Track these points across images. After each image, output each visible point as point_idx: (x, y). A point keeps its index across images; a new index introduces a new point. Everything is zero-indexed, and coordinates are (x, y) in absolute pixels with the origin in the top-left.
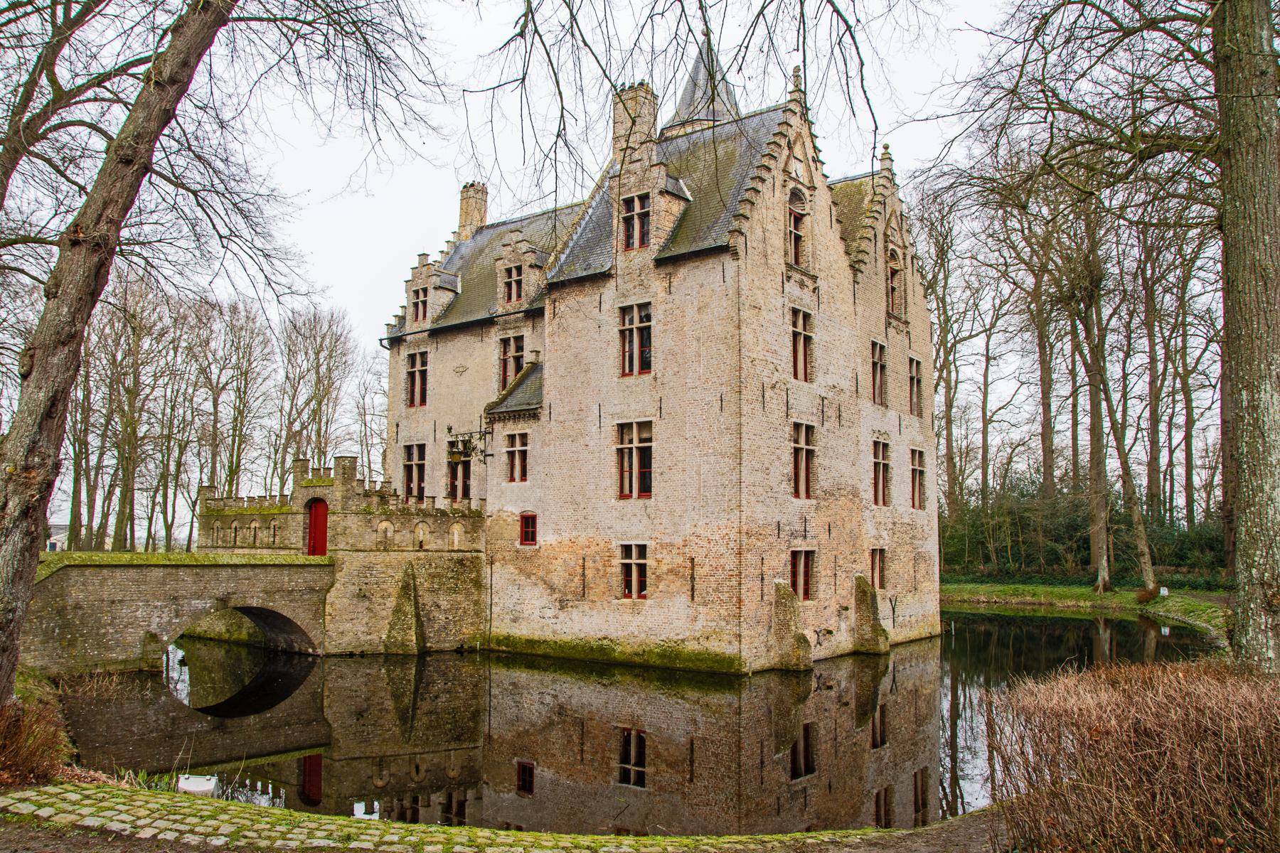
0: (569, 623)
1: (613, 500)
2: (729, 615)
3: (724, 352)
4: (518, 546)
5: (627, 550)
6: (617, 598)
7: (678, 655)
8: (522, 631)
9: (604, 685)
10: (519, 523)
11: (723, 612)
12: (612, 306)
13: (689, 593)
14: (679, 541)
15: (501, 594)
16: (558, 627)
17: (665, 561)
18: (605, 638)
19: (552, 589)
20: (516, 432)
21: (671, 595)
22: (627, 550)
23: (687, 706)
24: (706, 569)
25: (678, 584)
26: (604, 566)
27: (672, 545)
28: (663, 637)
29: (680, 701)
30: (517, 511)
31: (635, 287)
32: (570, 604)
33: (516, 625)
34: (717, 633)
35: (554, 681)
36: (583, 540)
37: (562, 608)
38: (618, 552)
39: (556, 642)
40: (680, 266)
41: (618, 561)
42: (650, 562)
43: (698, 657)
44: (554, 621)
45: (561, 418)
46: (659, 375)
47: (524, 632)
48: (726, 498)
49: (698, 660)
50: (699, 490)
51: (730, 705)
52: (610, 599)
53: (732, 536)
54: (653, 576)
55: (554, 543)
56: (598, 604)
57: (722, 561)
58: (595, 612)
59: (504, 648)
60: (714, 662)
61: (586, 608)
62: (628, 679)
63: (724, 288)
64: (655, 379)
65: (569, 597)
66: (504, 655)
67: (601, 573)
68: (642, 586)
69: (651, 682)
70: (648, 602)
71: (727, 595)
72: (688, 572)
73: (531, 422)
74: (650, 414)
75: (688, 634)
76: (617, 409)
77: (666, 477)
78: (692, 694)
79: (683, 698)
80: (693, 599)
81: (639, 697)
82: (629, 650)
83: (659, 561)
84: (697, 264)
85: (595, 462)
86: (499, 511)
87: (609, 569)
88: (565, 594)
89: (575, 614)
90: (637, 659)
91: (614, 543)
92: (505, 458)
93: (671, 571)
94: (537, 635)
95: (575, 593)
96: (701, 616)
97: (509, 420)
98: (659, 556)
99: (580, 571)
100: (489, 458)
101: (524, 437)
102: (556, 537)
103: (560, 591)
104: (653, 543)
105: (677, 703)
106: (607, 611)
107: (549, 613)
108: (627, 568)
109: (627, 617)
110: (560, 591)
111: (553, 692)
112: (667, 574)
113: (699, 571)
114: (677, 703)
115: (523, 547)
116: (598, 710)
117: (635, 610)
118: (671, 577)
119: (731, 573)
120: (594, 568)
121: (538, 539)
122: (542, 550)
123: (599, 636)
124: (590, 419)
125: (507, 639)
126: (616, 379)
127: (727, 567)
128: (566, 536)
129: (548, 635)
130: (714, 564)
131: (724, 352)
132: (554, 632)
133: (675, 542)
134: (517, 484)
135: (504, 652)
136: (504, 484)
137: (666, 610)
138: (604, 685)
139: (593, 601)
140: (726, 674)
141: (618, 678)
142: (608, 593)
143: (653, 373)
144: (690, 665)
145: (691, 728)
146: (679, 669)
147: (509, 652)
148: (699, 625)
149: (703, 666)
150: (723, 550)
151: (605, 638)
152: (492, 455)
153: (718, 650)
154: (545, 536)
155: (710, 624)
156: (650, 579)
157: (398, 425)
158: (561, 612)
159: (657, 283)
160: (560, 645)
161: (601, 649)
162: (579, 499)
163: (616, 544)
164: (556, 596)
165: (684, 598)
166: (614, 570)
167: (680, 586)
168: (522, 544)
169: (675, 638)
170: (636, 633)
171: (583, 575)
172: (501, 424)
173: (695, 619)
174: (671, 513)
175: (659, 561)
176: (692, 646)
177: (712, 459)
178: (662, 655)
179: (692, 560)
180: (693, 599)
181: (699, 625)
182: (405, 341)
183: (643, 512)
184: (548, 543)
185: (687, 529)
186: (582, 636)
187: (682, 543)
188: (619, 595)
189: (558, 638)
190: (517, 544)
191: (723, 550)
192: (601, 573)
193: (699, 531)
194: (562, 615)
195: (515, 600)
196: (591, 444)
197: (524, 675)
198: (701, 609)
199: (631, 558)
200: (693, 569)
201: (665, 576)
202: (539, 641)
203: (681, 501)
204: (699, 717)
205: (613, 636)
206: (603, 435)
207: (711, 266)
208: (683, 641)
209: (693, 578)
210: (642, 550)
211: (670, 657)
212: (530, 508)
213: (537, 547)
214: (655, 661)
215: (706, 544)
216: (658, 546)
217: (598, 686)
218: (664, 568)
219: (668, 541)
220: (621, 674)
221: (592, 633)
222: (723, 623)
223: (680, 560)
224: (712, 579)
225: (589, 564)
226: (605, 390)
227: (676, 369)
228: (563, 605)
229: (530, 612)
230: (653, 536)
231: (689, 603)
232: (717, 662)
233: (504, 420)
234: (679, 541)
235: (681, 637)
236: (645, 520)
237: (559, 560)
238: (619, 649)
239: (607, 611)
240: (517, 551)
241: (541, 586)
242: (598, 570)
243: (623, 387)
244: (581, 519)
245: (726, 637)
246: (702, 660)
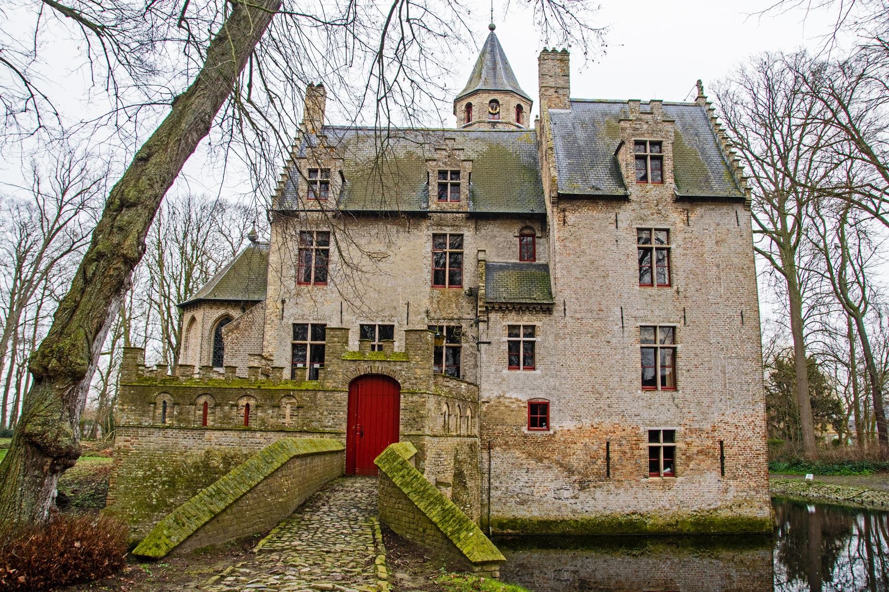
0: (592, 502)
1: (639, 391)
2: (758, 486)
3: (742, 279)
4: (526, 432)
5: (653, 435)
6: (646, 477)
7: (711, 523)
8: (533, 513)
9: (634, 555)
10: (527, 410)
11: (752, 484)
12: (630, 226)
13: (719, 470)
14: (707, 427)
15: (503, 478)
16: (579, 507)
17: (694, 444)
18: (633, 514)
19: (571, 471)
20: (522, 323)
21: (702, 472)
22: (653, 435)
23: (721, 564)
24: (735, 450)
25: (709, 462)
26: (631, 448)
27: (701, 430)
28: (695, 508)
29: (713, 561)
30: (525, 398)
31: (652, 214)
32: (592, 485)
33: (525, 507)
34: (750, 502)
35: (574, 558)
36: (607, 425)
37: (582, 489)
38: (647, 436)
39: (577, 521)
40: (697, 205)
41: (645, 445)
42: (679, 445)
43: (732, 523)
44: (573, 501)
45: (578, 316)
46: (681, 289)
47: (536, 514)
48: (750, 393)
49: (732, 524)
50: (725, 386)
51: (763, 559)
52: (637, 478)
53: (757, 423)
54: (684, 457)
55: (573, 428)
56: (625, 483)
57: (749, 443)
58: (621, 491)
59: (510, 531)
60: (747, 525)
61: (612, 487)
62: (661, 547)
63: (738, 230)
64: (678, 292)
65: (591, 478)
66: (510, 538)
67: (629, 455)
68: (670, 463)
69: (684, 547)
70: (679, 479)
71: (756, 470)
72: (717, 453)
73: (541, 316)
74: (675, 320)
75: (719, 503)
76: (641, 313)
77: (693, 373)
78: (725, 554)
79: (717, 558)
80: (723, 473)
81: (673, 563)
82: (661, 522)
83: (688, 444)
84: (712, 207)
85: (618, 357)
86: (499, 397)
87: (636, 452)
88: (587, 476)
89: (598, 494)
90: (670, 529)
91: (642, 429)
92: (506, 347)
93: (700, 452)
94: (553, 515)
95: (598, 474)
96: (731, 488)
97: (510, 311)
98: (689, 440)
99: (603, 453)
100: (483, 347)
101: (531, 330)
102: (575, 423)
103: (579, 473)
104: (682, 429)
105: (711, 563)
106: (635, 488)
107: (566, 494)
108: (654, 452)
109: (657, 493)
110: (579, 473)
111: (572, 568)
112: (697, 454)
113: (728, 452)
114: (711, 563)
115: (532, 432)
116: (627, 579)
117: (665, 486)
118: (701, 457)
119: (758, 452)
120: (620, 451)
121: (551, 424)
122: (557, 436)
123: (627, 512)
124: (611, 319)
125: (513, 523)
126: (637, 288)
127: (754, 448)
128: (587, 423)
129: (567, 515)
130: (742, 446)
131: (742, 279)
132: (574, 512)
133: (704, 428)
134: (521, 372)
135: (509, 535)
136: (506, 371)
137: (697, 485)
138: (634, 555)
139: (619, 481)
140: (758, 534)
141: (651, 547)
142: (636, 473)
143: (675, 288)
144: (725, 529)
145: (726, 582)
146: (714, 534)
147: (517, 535)
148: (730, 496)
149: (736, 530)
150: (750, 434)
151: (633, 514)
152: (489, 343)
153: (750, 515)
154: (560, 422)
155: (740, 494)
156: (679, 459)
157: (283, 302)
158: (581, 493)
159: (676, 215)
160: (582, 524)
161: (631, 524)
162: (602, 389)
163: (643, 430)
164: (575, 478)
165: (715, 474)
166: (642, 452)
167: (710, 464)
168: (529, 429)
169: (707, 508)
170: (668, 506)
171: (608, 458)
172: (500, 315)
173: (726, 491)
174: (699, 403)
175: (688, 444)
176: (725, 514)
177: (735, 361)
178: (697, 523)
179: (721, 443)
180: (723, 473)
181: (730, 496)
182: (297, 216)
183: (671, 402)
184: (566, 428)
185: (716, 417)
186: (608, 512)
187: (711, 429)
188: (647, 474)
189: (578, 517)
190: (525, 430)
191: (750, 434)
192: (629, 455)
193: (726, 419)
194: (582, 495)
195: (521, 484)
196: (614, 341)
197: (536, 555)
198: (731, 482)
199: (658, 441)
200: (722, 448)
201: (695, 456)
202: (555, 522)
203: (709, 394)
204: (733, 573)
205: (644, 510)
206: (626, 334)
207: (725, 211)
208: (715, 510)
209: (722, 458)
210: (670, 435)
211: (704, 525)
212: (540, 395)
213: (551, 432)
214: (687, 528)
215: (733, 429)
216: (687, 431)
217: (627, 557)
218: (695, 450)
219: (697, 427)
220: (653, 544)
221: (619, 510)
222: (753, 493)
223: (709, 443)
224: (740, 457)
225: (614, 447)
226: (626, 295)
227: (698, 287)
228: (583, 486)
229: (542, 494)
230: (682, 423)
231: (720, 478)
232: (750, 525)
233: (503, 311)
234: (707, 427)
235: (712, 507)
236: (673, 409)
237: (579, 444)
238: (651, 521)
239: (635, 488)
240: (526, 436)
241: (556, 470)
242: (624, 453)
243: (645, 295)
244: (606, 407)
245: (756, 504)
246: (735, 525)
